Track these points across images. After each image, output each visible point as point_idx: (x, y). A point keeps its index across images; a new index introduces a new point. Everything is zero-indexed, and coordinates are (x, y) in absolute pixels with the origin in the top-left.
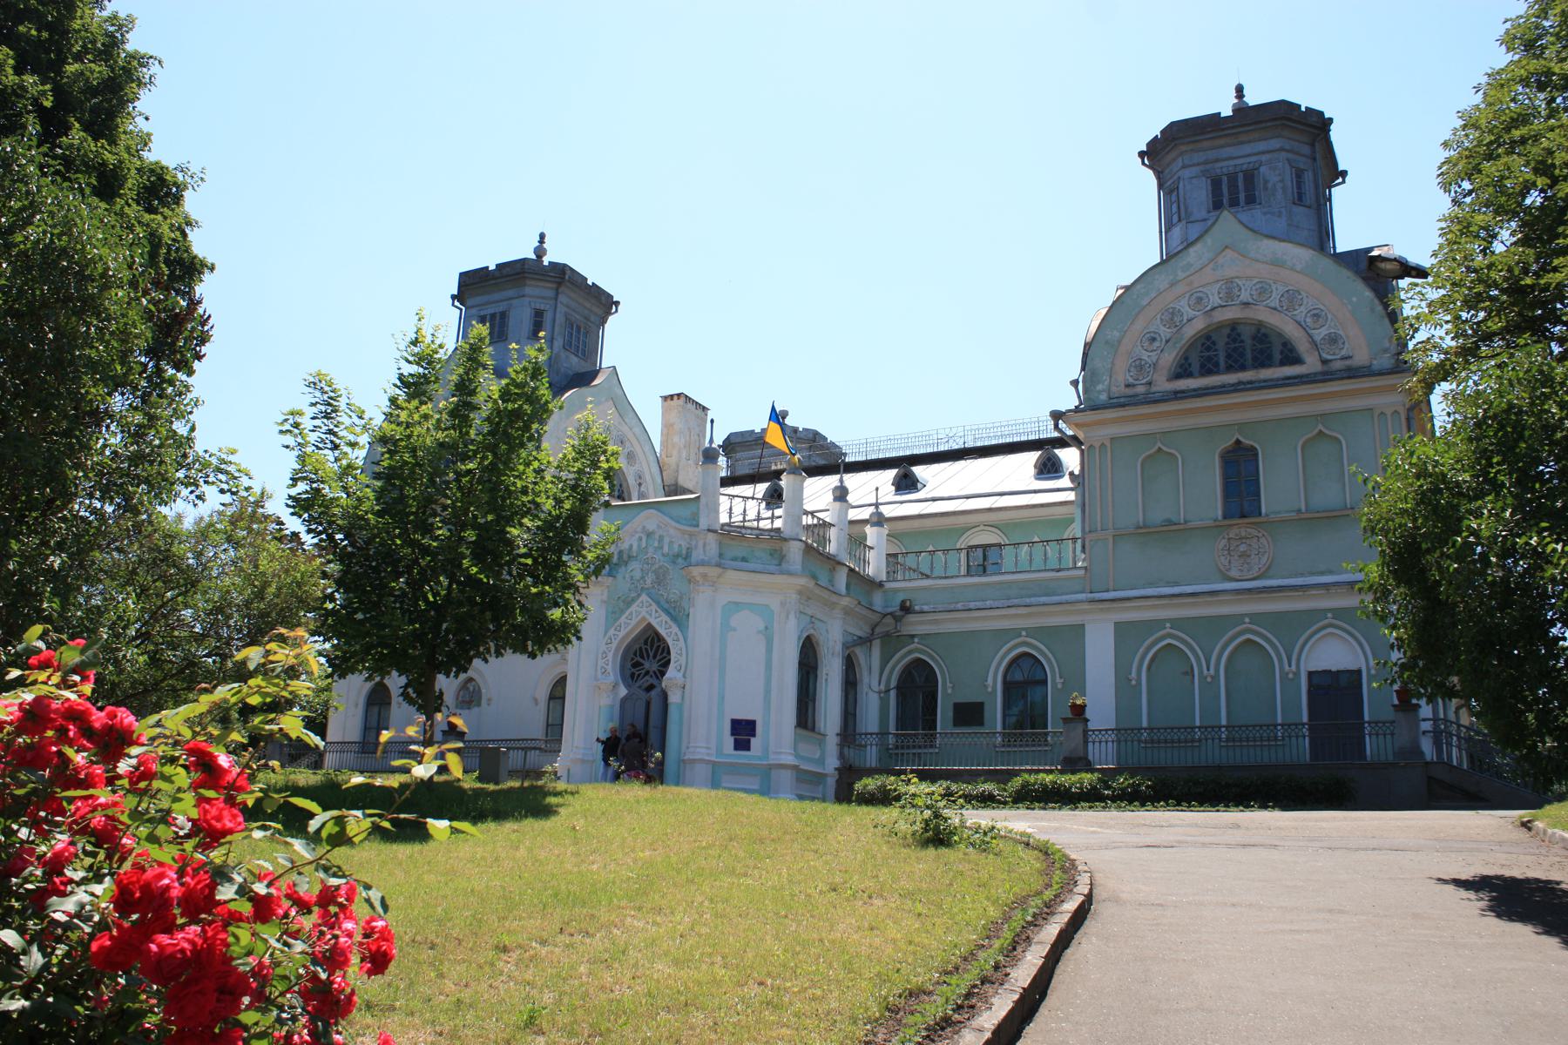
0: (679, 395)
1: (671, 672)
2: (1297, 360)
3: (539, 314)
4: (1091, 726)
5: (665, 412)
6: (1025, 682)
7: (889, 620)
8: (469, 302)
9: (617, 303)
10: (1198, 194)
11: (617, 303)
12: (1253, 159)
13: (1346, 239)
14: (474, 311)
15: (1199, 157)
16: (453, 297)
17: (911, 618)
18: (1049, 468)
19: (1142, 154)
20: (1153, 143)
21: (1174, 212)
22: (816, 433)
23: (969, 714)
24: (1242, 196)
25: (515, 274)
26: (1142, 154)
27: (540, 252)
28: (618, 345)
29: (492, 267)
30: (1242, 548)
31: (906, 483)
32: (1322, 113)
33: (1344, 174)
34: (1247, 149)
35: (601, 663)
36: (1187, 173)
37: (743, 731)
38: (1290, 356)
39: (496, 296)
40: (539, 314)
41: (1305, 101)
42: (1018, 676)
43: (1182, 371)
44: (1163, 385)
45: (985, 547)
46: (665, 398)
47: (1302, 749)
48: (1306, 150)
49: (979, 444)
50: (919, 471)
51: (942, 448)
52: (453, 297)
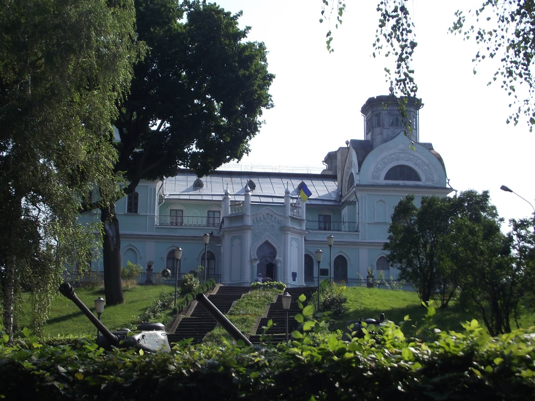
1: (277, 258)
13: (423, 139)
23: (324, 272)
35: (252, 253)
36: (384, 112)
37: (294, 275)
43: (387, 177)
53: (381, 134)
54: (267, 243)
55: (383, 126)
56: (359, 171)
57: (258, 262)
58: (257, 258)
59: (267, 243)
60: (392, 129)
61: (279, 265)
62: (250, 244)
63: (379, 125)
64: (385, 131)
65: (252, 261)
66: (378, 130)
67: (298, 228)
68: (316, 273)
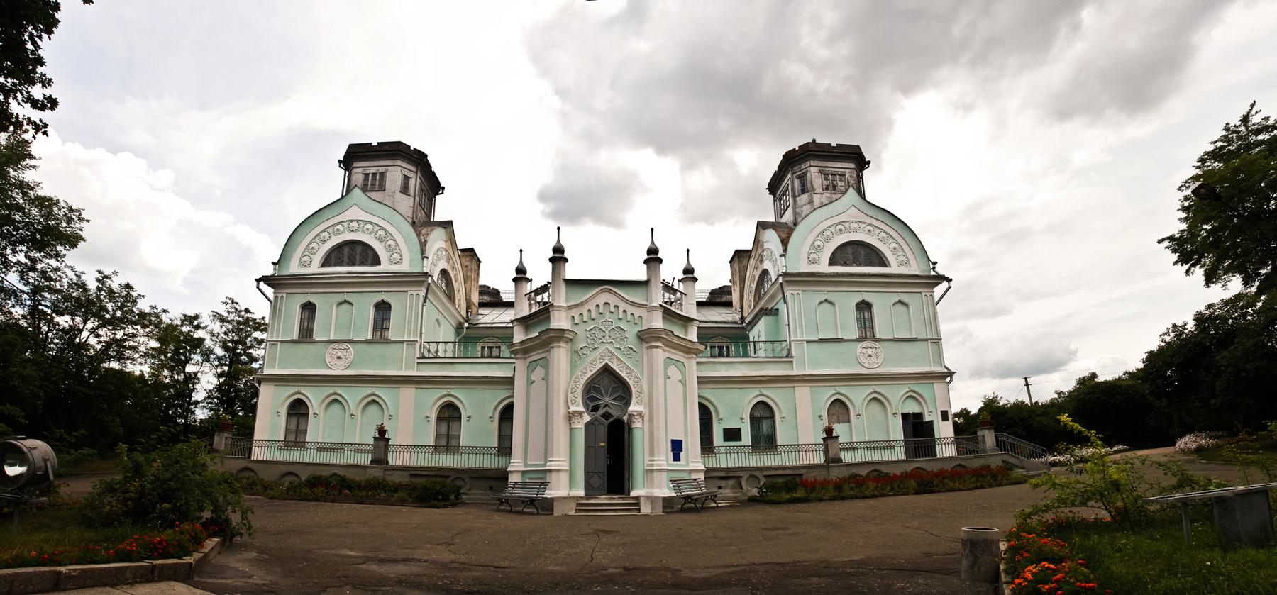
15: (820, 163)
23: (732, 435)
38: (883, 262)
39: (376, 163)
42: (757, 414)
44: (824, 267)
53: (811, 202)
54: (607, 370)
55: (813, 189)
56: (785, 251)
57: (587, 418)
58: (581, 408)
59: (607, 370)
60: (827, 194)
61: (637, 424)
62: (566, 376)
63: (803, 191)
64: (817, 199)
65: (571, 417)
66: (805, 197)
68: (718, 439)
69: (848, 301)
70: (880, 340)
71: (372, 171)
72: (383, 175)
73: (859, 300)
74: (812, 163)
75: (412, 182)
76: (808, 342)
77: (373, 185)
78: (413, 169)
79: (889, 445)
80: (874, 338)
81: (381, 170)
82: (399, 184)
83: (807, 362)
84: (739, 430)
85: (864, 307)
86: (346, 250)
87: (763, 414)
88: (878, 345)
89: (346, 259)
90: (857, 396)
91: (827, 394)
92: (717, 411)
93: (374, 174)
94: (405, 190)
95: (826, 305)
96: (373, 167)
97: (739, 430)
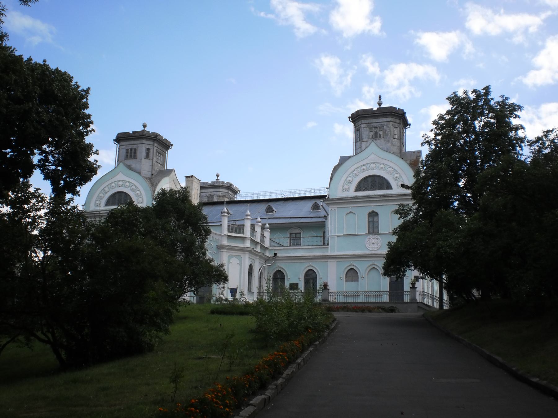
0: (192, 176)
2: (391, 188)
3: (148, 150)
4: (330, 291)
5: (186, 181)
6: (310, 277)
7: (271, 259)
8: (122, 143)
9: (172, 145)
10: (366, 132)
11: (172, 145)
12: (382, 123)
14: (124, 147)
16: (114, 140)
17: (277, 258)
18: (316, 207)
19: (349, 118)
20: (353, 115)
21: (359, 139)
22: (231, 185)
24: (378, 135)
25: (141, 136)
26: (349, 118)
27: (145, 126)
28: (172, 159)
29: (131, 132)
30: (373, 241)
31: (270, 210)
32: (403, 110)
33: (410, 125)
34: (381, 120)
36: (362, 126)
38: (389, 187)
40: (148, 150)
41: (398, 106)
43: (358, 189)
44: (352, 193)
45: (296, 234)
46: (187, 177)
47: (386, 299)
48: (398, 121)
49: (292, 196)
50: (272, 205)
51: (280, 197)
52: (114, 140)
67: (242, 245)
69: (363, 212)
70: (380, 234)
71: (130, 147)
72: (135, 150)
73: (370, 210)
74: (363, 121)
75: (151, 151)
76: (338, 236)
77: (131, 156)
78: (152, 143)
79: (379, 294)
80: (377, 233)
81: (135, 146)
82: (144, 154)
83: (336, 247)
84: (297, 285)
85: (373, 215)
86: (117, 196)
87: (310, 277)
88: (379, 237)
89: (117, 201)
90: (362, 267)
91: (345, 265)
92: (287, 275)
93: (131, 149)
94: (147, 156)
95: (351, 214)
96: (130, 145)
97: (297, 285)
